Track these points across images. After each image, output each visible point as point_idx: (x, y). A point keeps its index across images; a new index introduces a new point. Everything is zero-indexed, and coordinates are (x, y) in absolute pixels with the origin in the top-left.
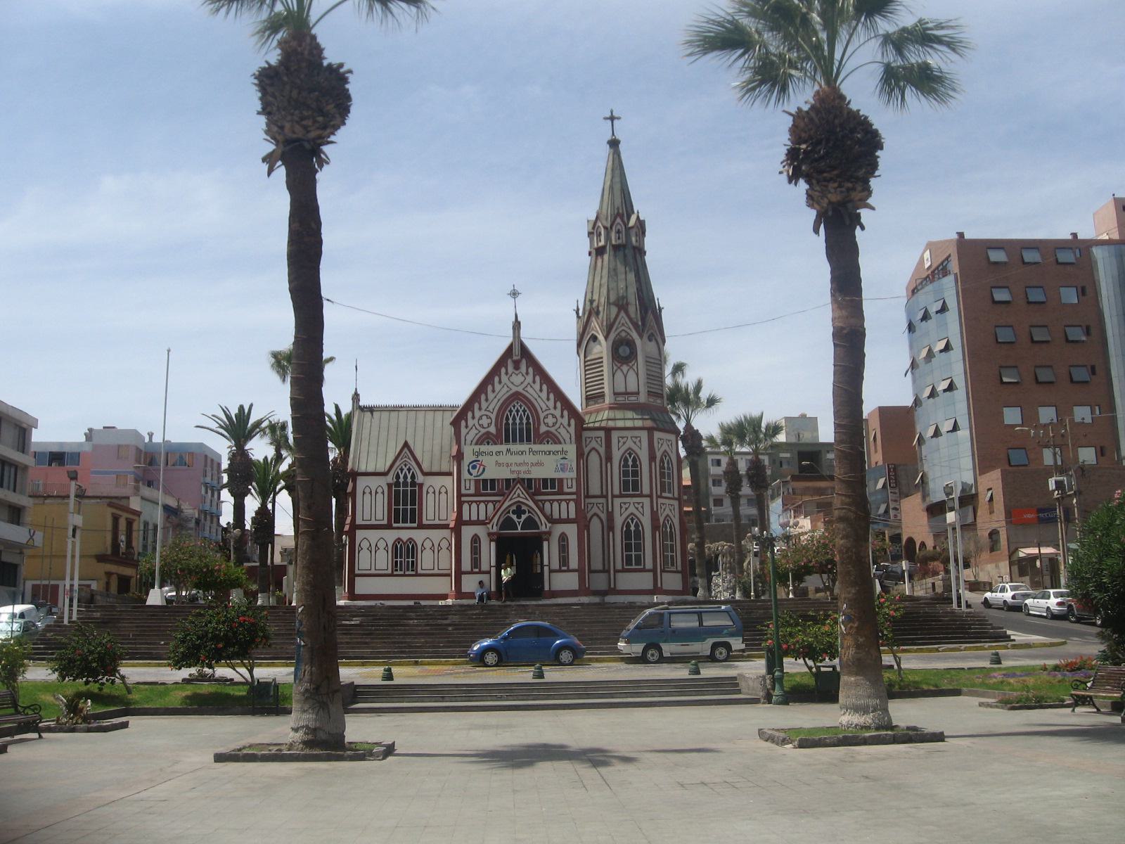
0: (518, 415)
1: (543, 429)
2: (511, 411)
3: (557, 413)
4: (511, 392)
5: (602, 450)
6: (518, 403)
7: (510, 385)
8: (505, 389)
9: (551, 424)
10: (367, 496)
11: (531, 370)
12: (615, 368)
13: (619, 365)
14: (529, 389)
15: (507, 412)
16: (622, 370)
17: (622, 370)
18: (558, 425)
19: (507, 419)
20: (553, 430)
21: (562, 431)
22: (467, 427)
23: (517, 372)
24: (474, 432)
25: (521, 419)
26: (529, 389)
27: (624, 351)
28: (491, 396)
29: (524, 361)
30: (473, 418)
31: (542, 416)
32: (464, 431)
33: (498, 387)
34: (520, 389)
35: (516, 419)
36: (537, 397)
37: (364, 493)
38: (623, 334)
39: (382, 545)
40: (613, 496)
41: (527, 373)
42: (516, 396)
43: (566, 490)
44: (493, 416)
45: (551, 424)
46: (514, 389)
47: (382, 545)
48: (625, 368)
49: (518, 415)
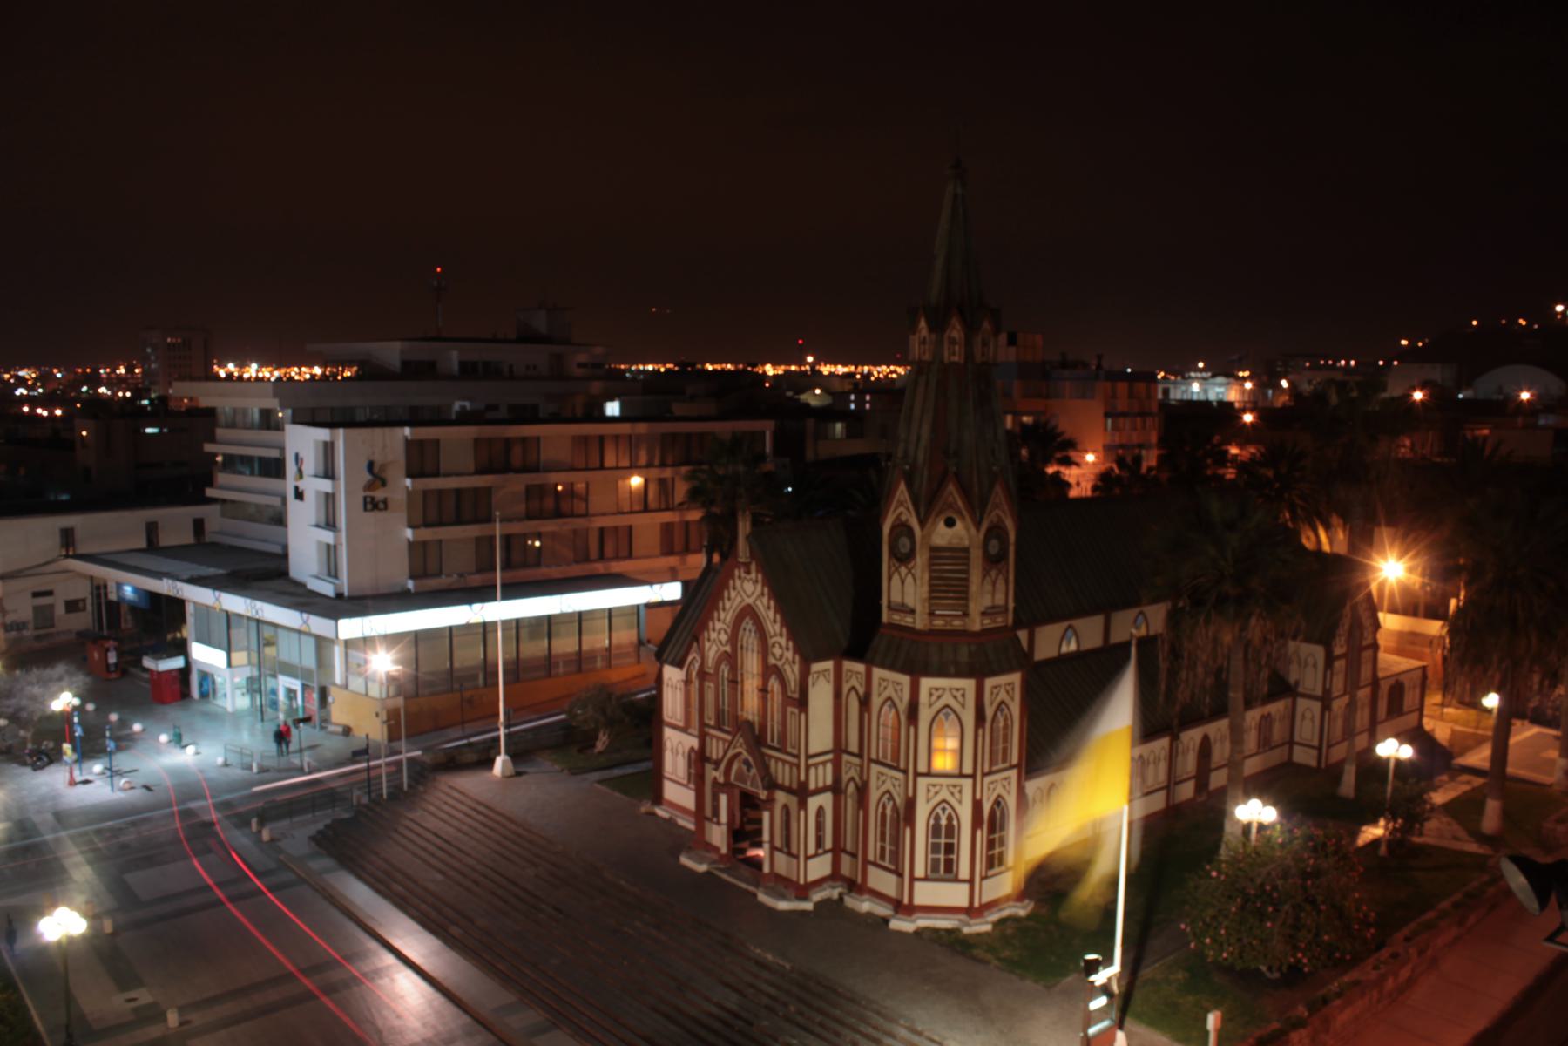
1: (772, 661)
3: (783, 641)
4: (743, 604)
5: (861, 691)
8: (739, 599)
9: (778, 657)
12: (893, 569)
13: (897, 564)
14: (758, 603)
16: (900, 574)
17: (900, 574)
18: (784, 660)
20: (779, 663)
21: (787, 668)
22: (709, 640)
23: (748, 577)
24: (714, 648)
27: (904, 544)
28: (728, 605)
30: (714, 630)
31: (771, 641)
32: (707, 645)
33: (733, 594)
34: (750, 601)
36: (765, 615)
38: (903, 518)
39: (680, 750)
40: (870, 760)
42: (748, 612)
43: (790, 750)
44: (729, 631)
45: (778, 657)
47: (680, 750)
48: (903, 570)
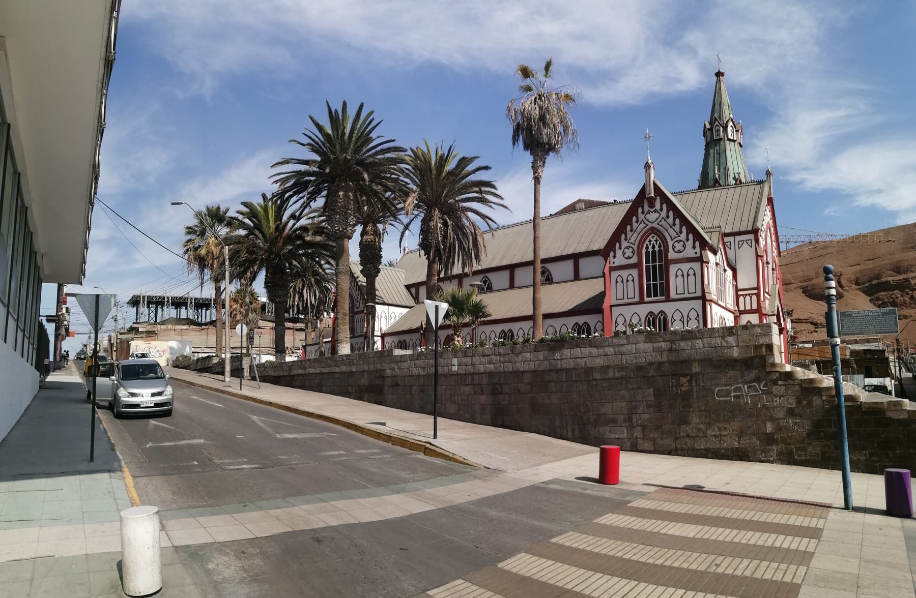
0: (650, 244)
2: (650, 241)
6: (653, 237)
7: (646, 222)
10: (620, 285)
11: (664, 206)
15: (647, 242)
19: (647, 247)
25: (653, 247)
26: (663, 223)
29: (658, 200)
34: (655, 225)
35: (655, 247)
37: (617, 282)
41: (661, 210)
42: (653, 230)
46: (650, 225)
49: (650, 244)
